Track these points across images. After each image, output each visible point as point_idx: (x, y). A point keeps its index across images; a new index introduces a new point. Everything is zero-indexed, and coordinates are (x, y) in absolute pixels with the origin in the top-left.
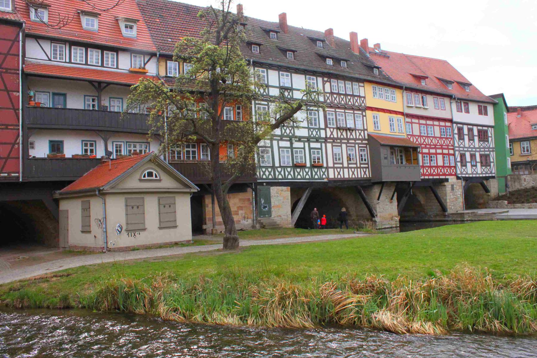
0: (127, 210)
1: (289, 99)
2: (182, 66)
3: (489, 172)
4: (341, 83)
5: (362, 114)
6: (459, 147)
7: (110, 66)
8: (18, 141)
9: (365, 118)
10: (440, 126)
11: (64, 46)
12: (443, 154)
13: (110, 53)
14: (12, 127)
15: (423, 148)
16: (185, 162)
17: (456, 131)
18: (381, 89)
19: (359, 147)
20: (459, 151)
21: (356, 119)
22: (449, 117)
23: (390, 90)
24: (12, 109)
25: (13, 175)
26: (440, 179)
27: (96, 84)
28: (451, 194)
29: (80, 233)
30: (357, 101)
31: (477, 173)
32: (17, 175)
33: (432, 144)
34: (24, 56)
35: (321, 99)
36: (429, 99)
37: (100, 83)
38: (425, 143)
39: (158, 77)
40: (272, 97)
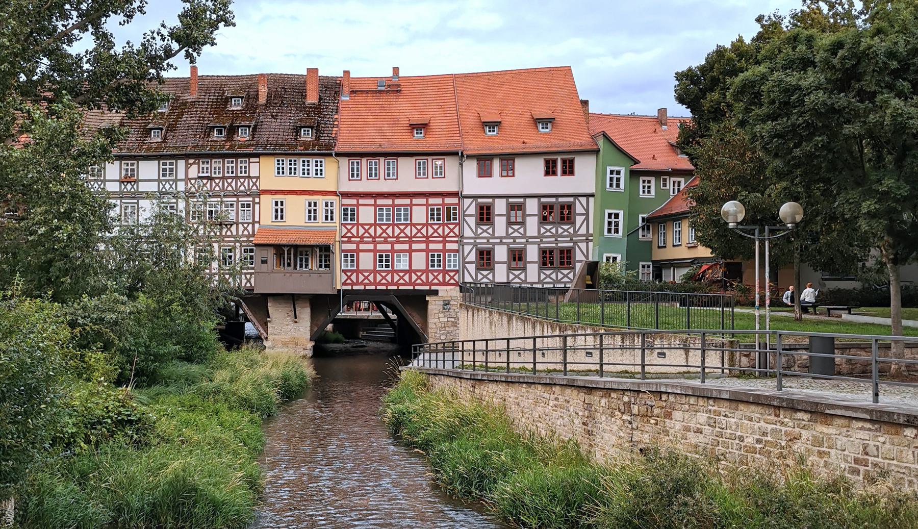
1: (133, 193)
3: (566, 280)
4: (216, 164)
5: (253, 201)
6: (477, 236)
9: (257, 206)
10: (427, 205)
12: (427, 250)
15: (380, 243)
17: (472, 210)
18: (295, 161)
19: (241, 246)
20: (475, 244)
21: (240, 208)
22: (454, 188)
23: (313, 161)
26: (414, 290)
28: (441, 315)
30: (242, 184)
31: (525, 282)
33: (402, 235)
35: (181, 186)
36: (406, 166)
38: (384, 235)
40: (109, 193)
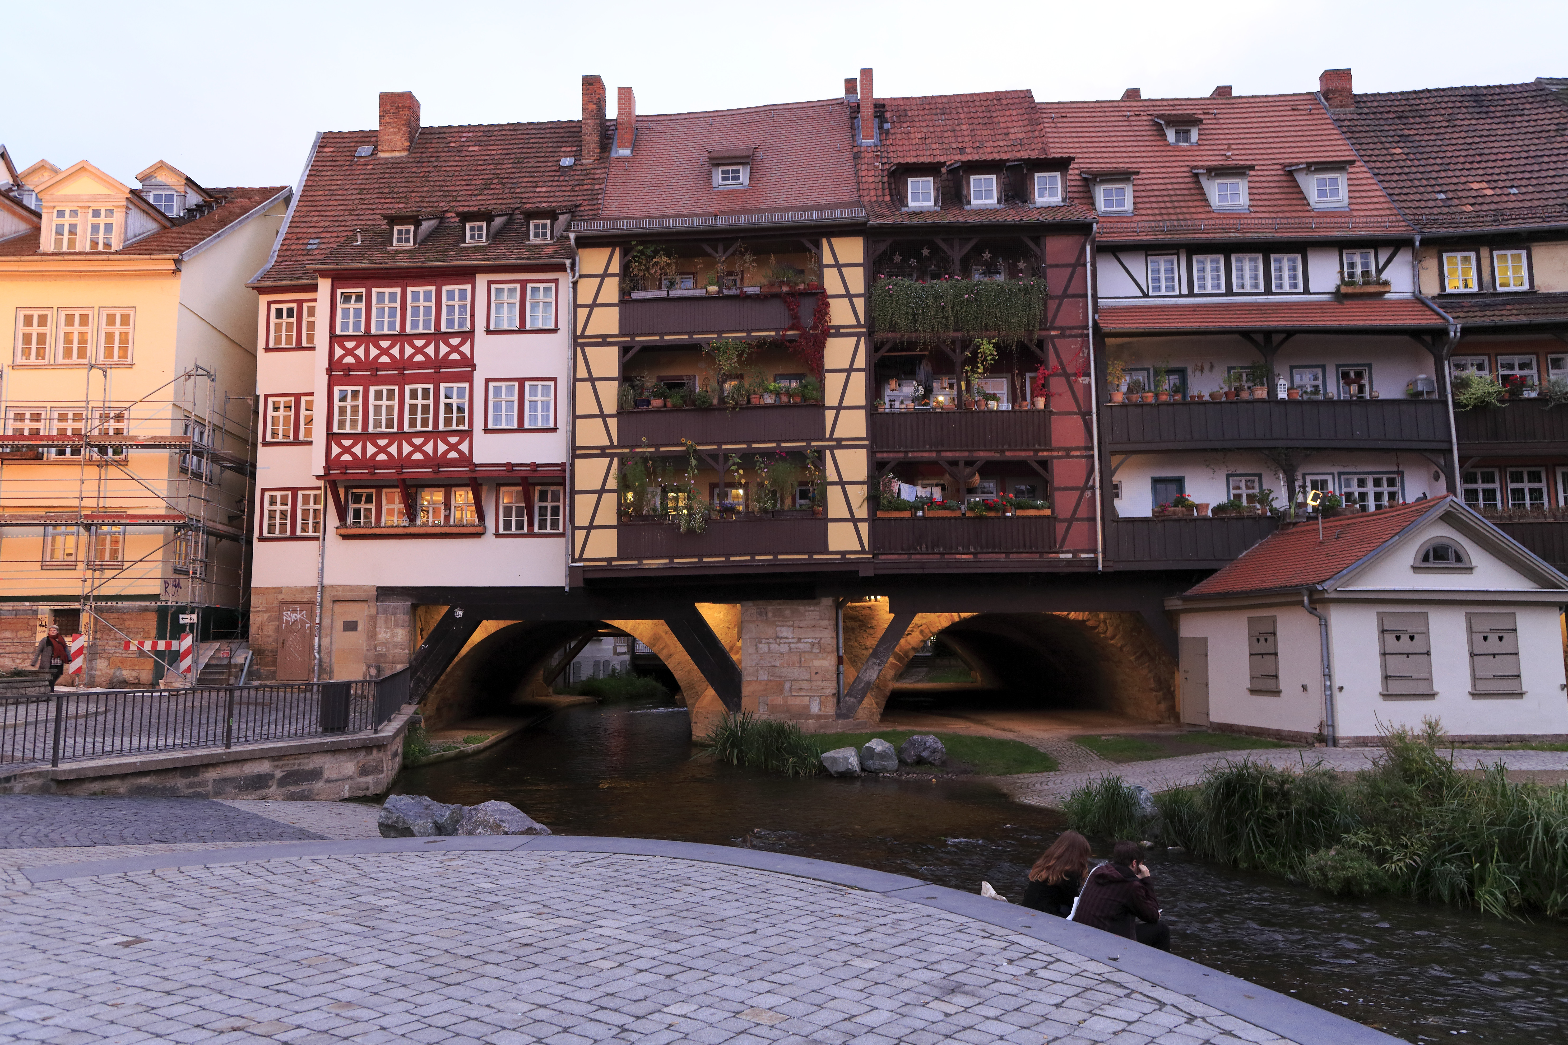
0: (1383, 643)
2: (1489, 260)
7: (1248, 289)
8: (1091, 483)
11: (1175, 258)
13: (1247, 257)
14: (1078, 453)
16: (1516, 521)
24: (1075, 414)
25: (1083, 556)
27: (1260, 338)
29: (1248, 693)
32: (1092, 556)
34: (1095, 297)
37: (1268, 334)
39: (1419, 299)
